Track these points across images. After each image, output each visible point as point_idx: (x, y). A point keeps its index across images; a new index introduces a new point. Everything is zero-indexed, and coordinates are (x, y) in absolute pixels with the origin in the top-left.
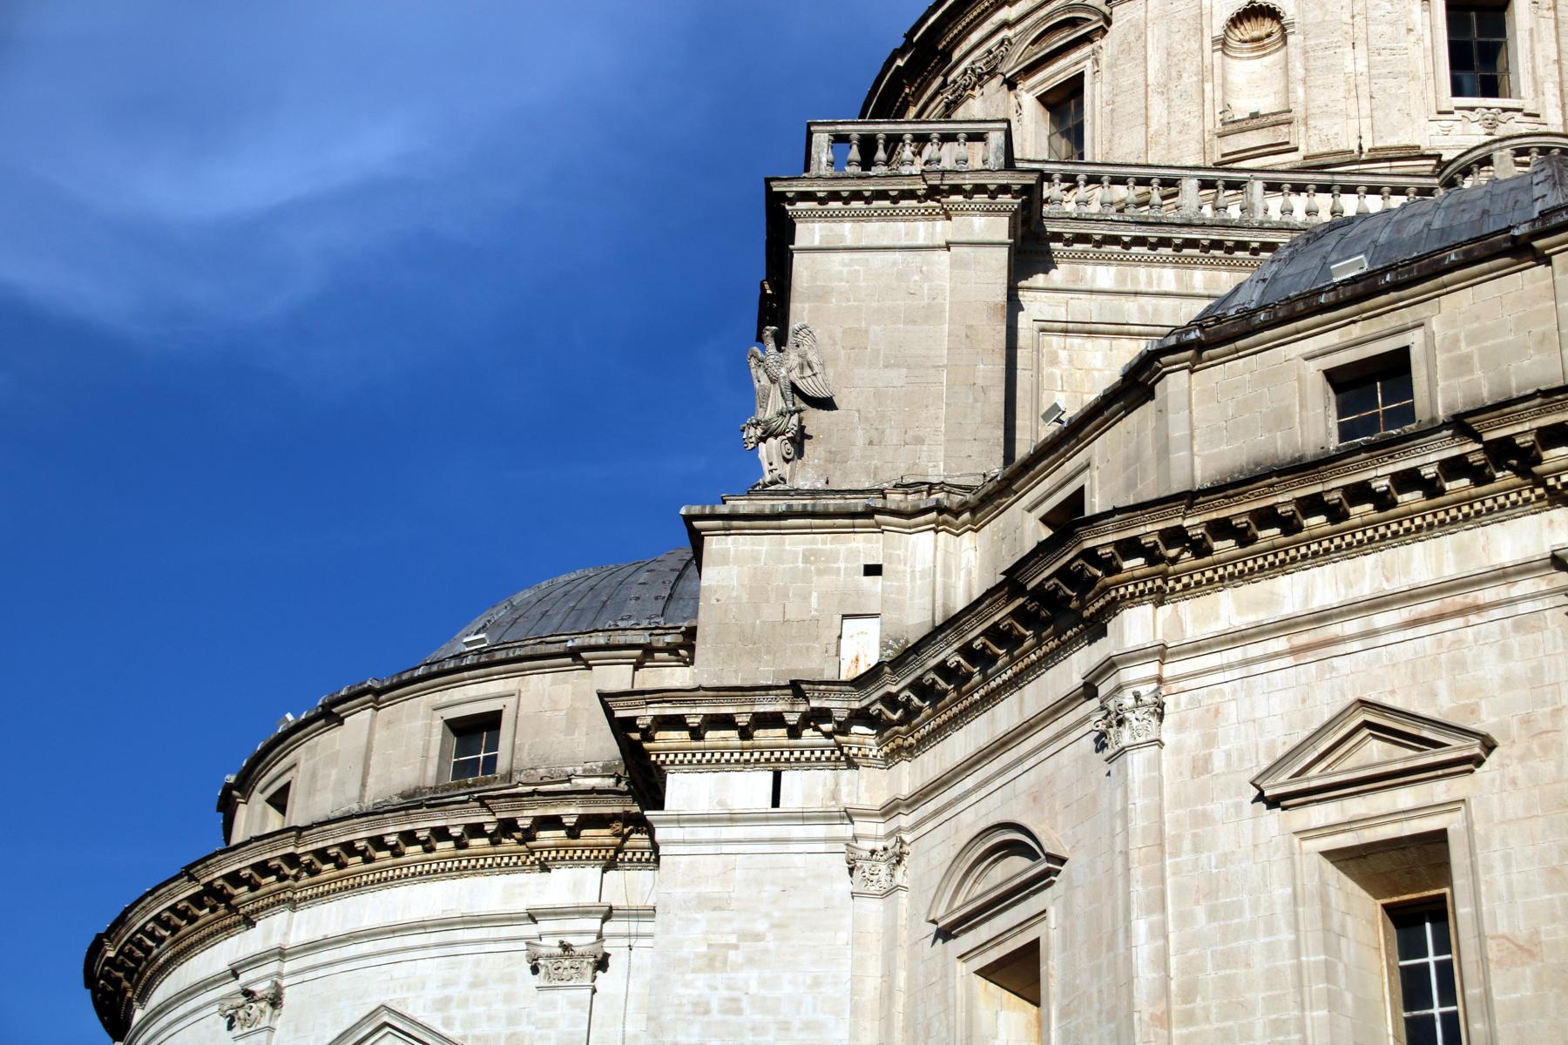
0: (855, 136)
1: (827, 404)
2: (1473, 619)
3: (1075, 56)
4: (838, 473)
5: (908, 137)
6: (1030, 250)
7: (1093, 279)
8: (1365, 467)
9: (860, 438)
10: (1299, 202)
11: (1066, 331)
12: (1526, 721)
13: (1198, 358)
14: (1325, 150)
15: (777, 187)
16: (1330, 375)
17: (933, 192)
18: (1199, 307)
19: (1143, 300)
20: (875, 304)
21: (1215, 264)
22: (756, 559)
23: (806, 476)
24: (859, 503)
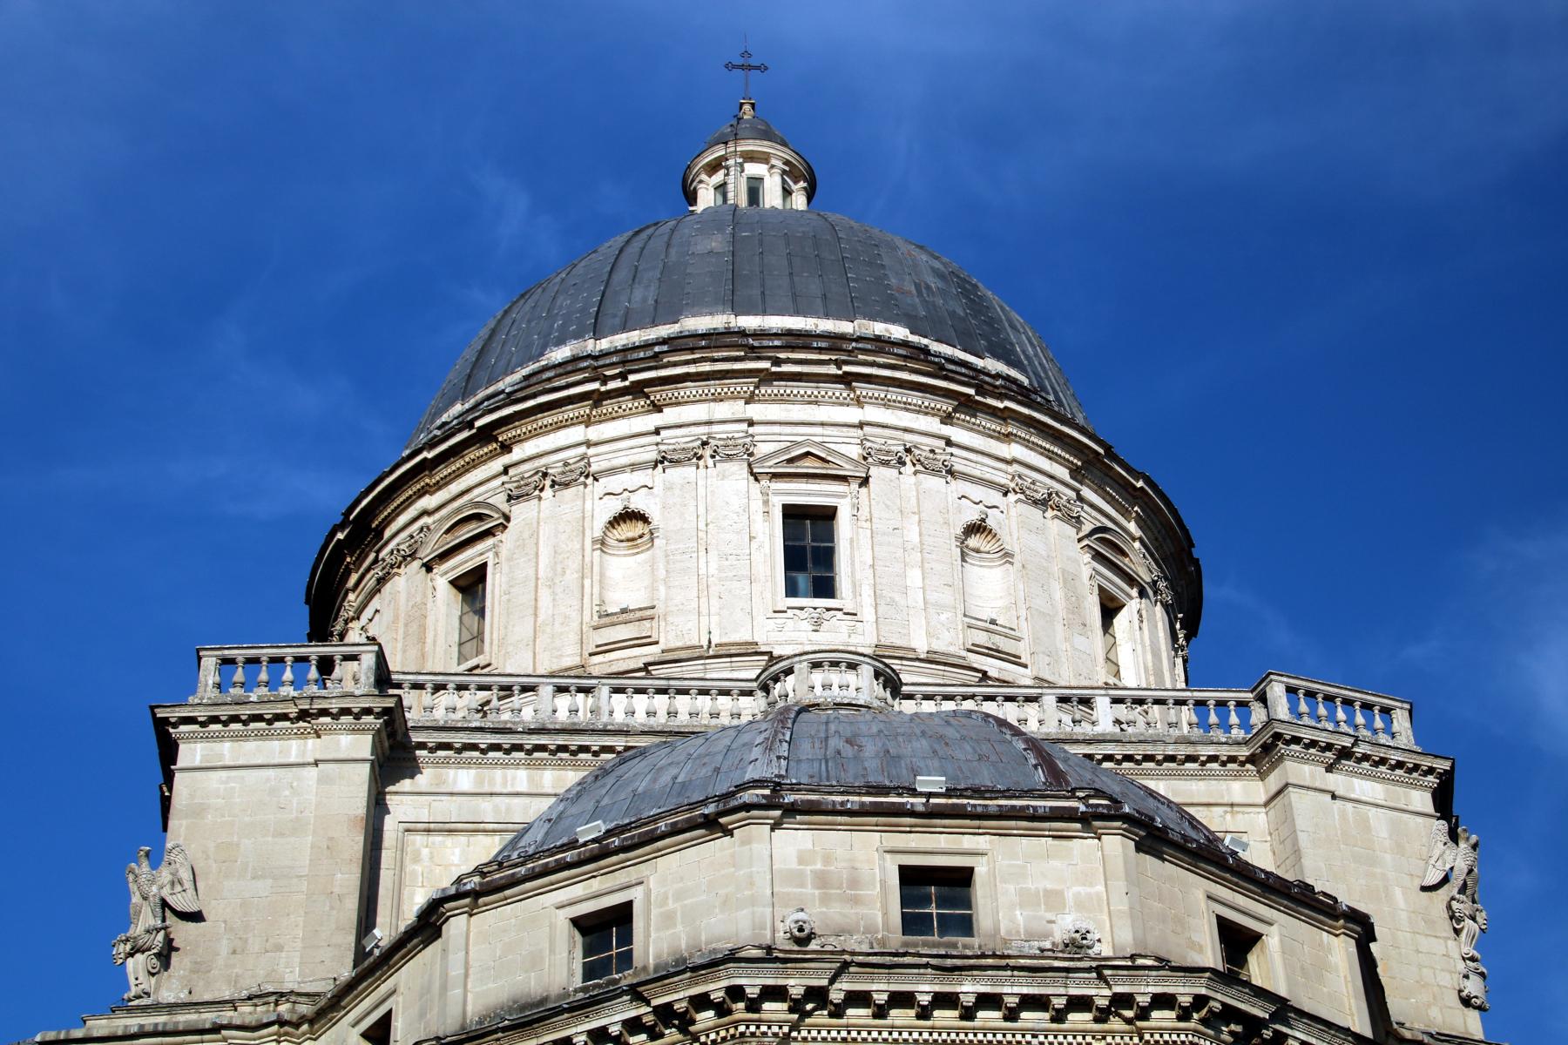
0: (240, 659)
1: (196, 917)
3: (480, 546)
4: (201, 983)
5: (289, 659)
6: (395, 756)
7: (455, 782)
8: (567, 1025)
9: (224, 948)
10: (641, 702)
11: (429, 831)
13: (475, 905)
14: (680, 644)
15: (161, 714)
16: (576, 922)
17: (304, 715)
18: (544, 805)
19: (495, 798)
20: (247, 819)
21: (562, 765)
23: (170, 989)
24: (208, 1017)
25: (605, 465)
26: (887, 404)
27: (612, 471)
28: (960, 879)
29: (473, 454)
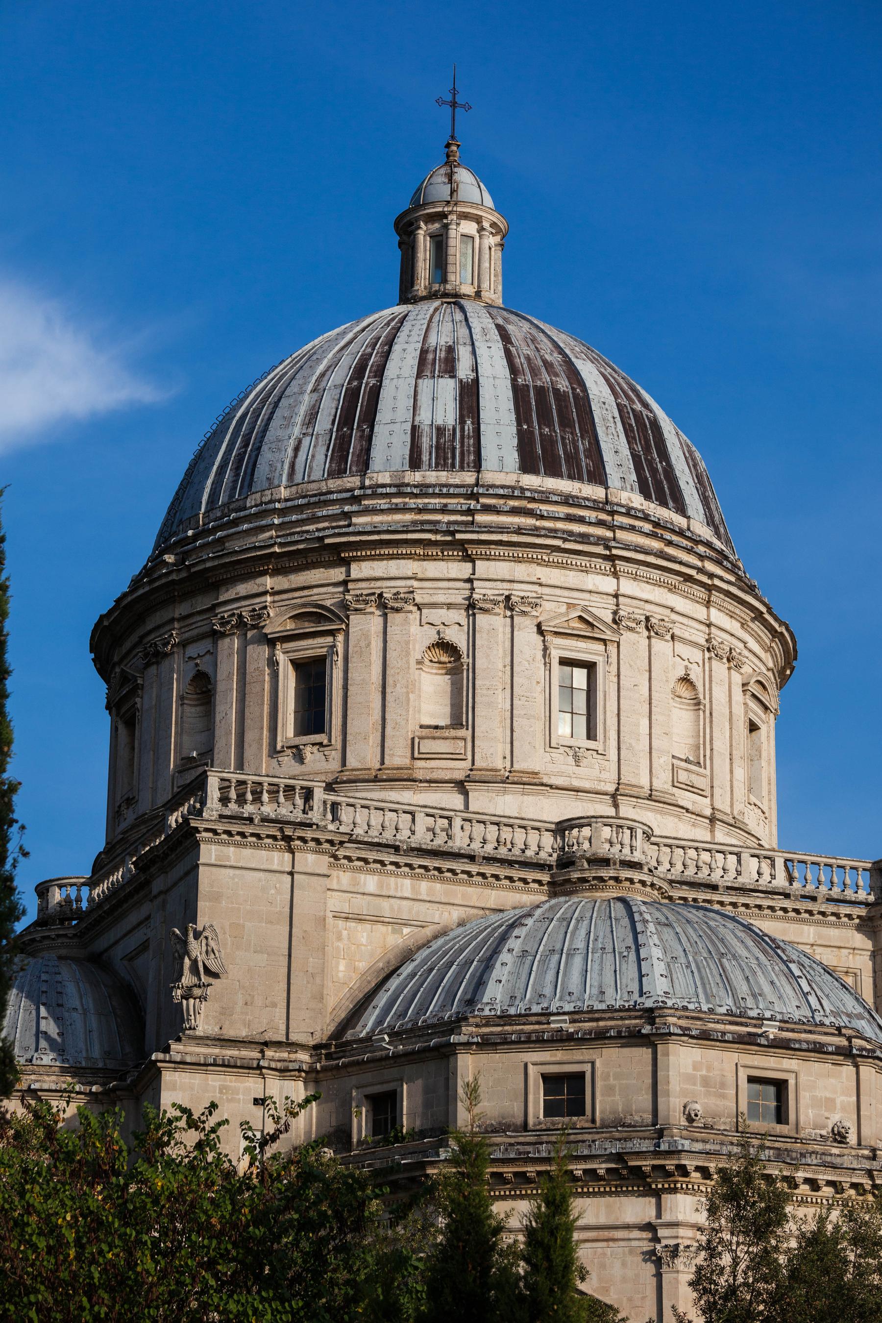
2: (611, 1244)
4: (227, 1022)
7: (365, 884)
11: (347, 918)
12: (630, 1299)
19: (392, 900)
21: (433, 878)
22: (192, 1089)
25: (427, 599)
26: (635, 578)
27: (433, 605)
28: (780, 1086)
29: (312, 557)
